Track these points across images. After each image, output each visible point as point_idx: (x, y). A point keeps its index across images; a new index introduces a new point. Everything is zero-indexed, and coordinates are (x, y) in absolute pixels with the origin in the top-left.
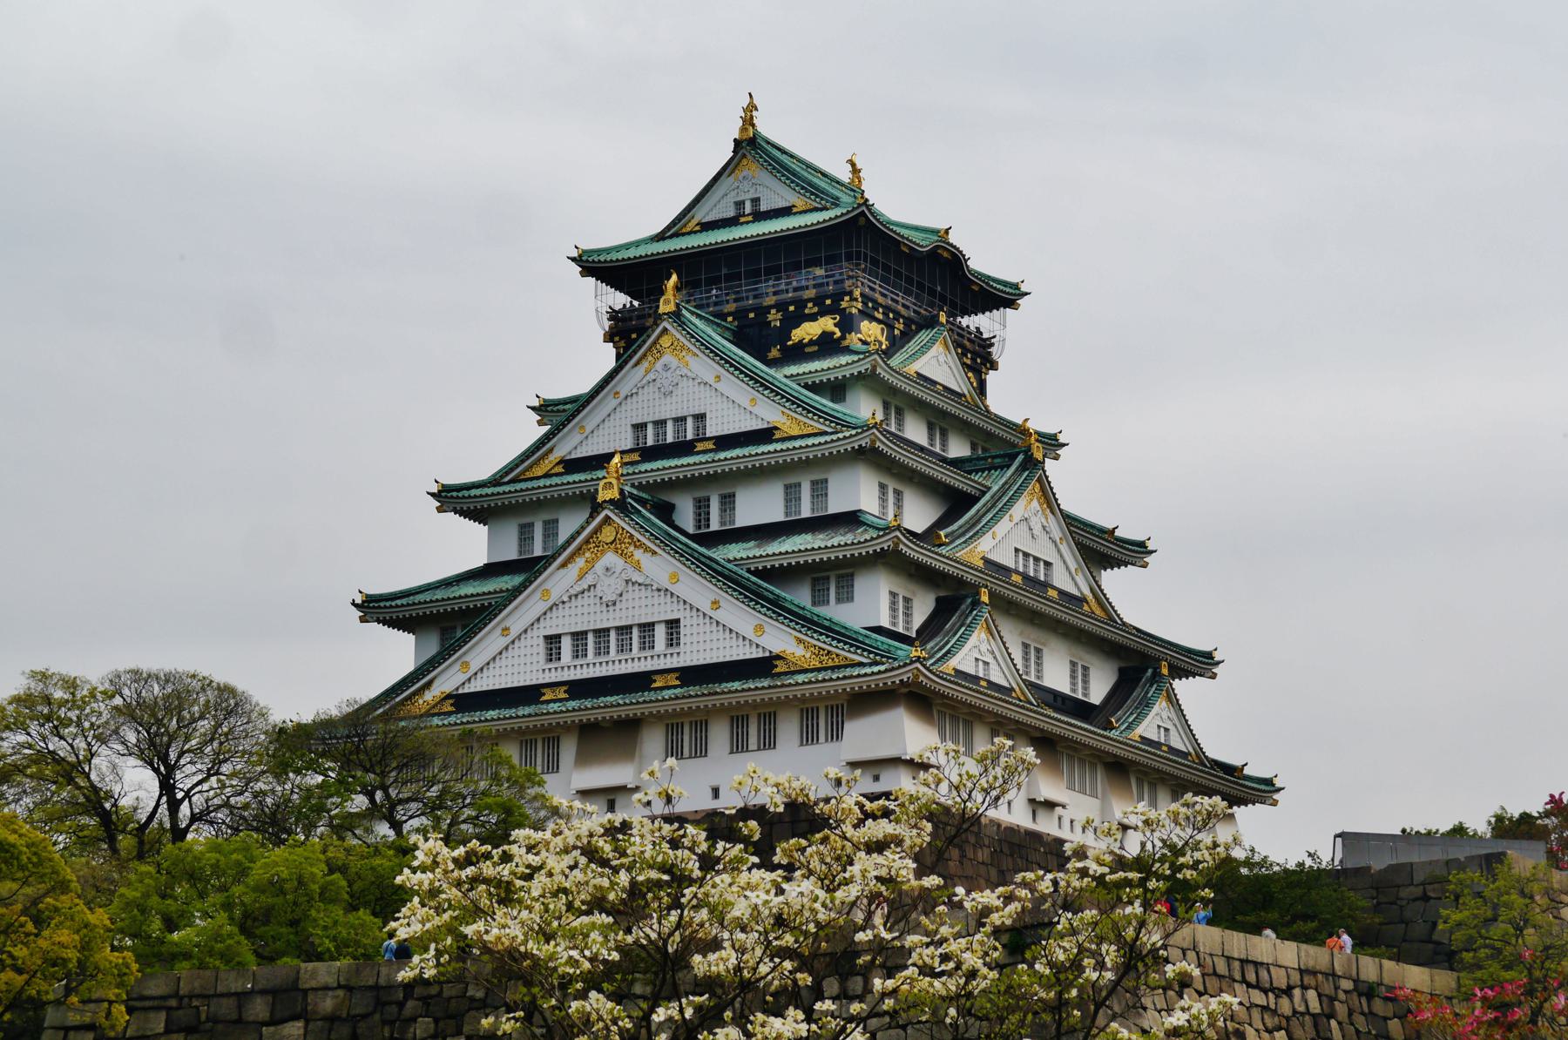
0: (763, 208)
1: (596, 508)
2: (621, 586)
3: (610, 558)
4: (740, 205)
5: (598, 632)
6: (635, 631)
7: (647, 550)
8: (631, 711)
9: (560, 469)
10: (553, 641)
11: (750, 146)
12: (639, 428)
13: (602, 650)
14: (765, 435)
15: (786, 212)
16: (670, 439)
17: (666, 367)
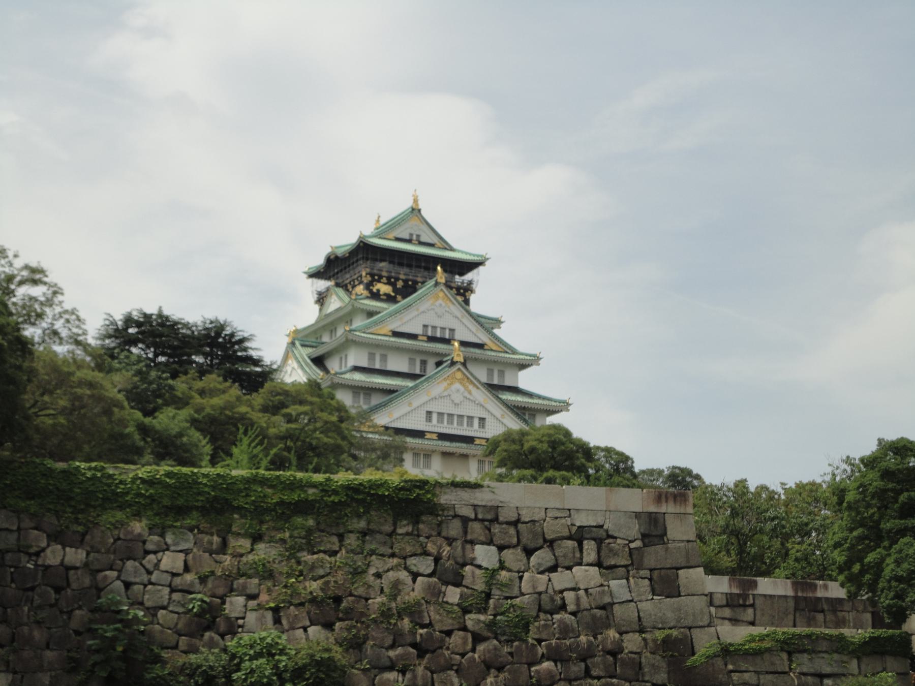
0: (423, 239)
1: (453, 363)
2: (462, 399)
3: (457, 386)
4: (411, 235)
5: (449, 415)
6: (465, 419)
7: (475, 385)
8: (465, 451)
9: (390, 334)
10: (429, 413)
11: (415, 211)
12: (425, 326)
13: (450, 422)
14: (481, 346)
15: (431, 245)
16: (438, 335)
17: (441, 305)
